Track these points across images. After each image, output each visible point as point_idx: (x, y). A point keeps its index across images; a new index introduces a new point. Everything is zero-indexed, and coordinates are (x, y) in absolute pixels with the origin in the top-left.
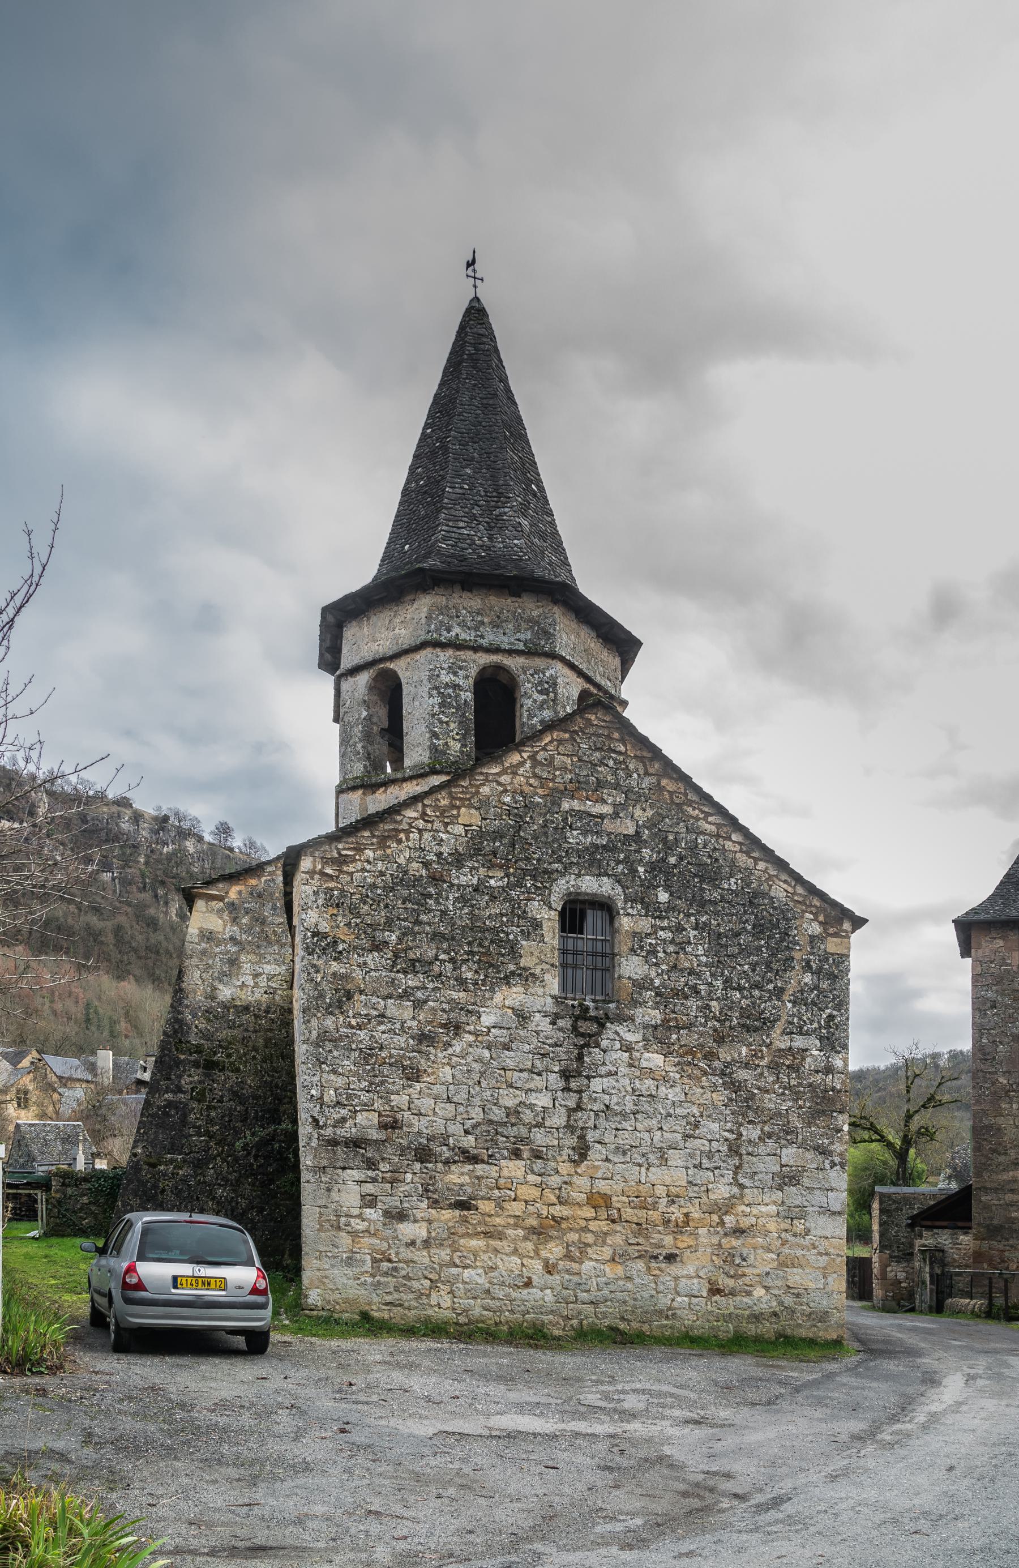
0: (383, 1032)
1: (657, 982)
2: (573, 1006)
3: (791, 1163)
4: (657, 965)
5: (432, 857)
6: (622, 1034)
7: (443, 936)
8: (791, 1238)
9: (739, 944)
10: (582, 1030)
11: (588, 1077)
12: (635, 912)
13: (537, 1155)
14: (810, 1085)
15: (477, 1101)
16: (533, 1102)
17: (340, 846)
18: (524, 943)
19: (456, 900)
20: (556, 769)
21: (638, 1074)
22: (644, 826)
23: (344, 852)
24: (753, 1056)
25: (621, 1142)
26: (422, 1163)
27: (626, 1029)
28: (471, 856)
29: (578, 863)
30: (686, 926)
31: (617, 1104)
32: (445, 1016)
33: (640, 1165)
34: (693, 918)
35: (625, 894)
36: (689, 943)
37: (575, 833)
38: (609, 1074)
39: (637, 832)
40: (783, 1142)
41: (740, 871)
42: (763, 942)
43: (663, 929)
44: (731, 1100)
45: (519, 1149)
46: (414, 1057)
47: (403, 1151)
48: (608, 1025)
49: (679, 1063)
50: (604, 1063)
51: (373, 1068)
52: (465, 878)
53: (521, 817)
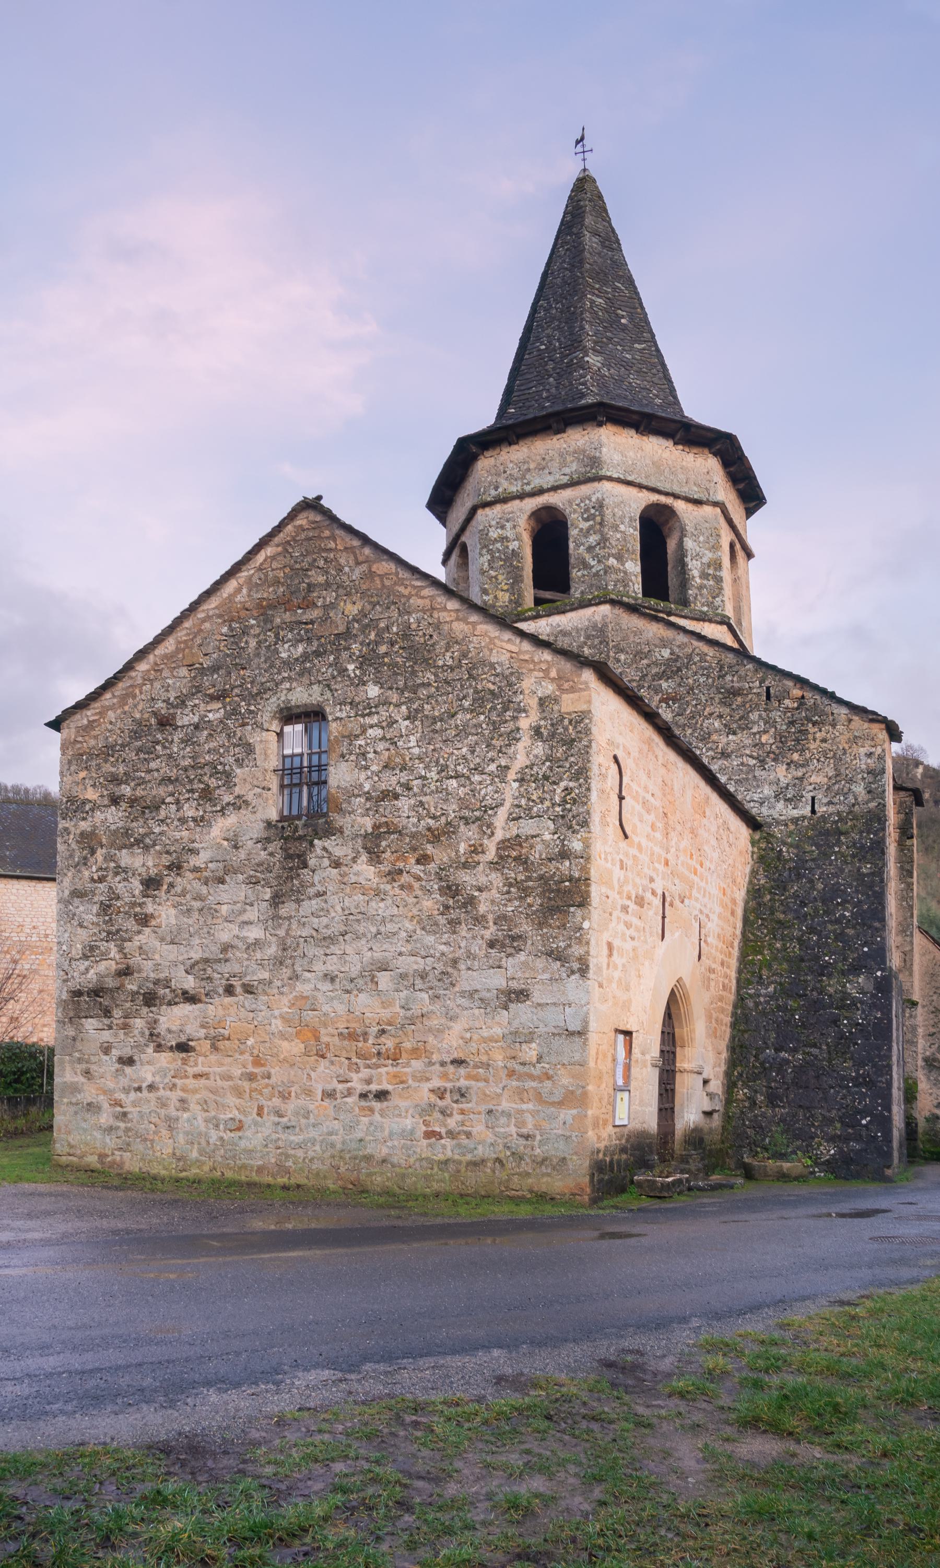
0: (119, 882)
1: (367, 787)
2: (283, 827)
3: (519, 974)
4: (366, 768)
5: (160, 704)
6: (330, 849)
7: (169, 779)
8: (518, 1068)
9: (457, 726)
10: (291, 852)
11: (298, 901)
12: (344, 715)
13: (249, 990)
14: (541, 877)
15: (196, 941)
16: (246, 934)
17: (89, 713)
18: (238, 771)
19: (182, 741)
20: (269, 587)
21: (348, 891)
22: (354, 620)
23: (91, 719)
24: (473, 852)
25: (330, 968)
26: (149, 1007)
27: (334, 843)
28: (193, 695)
29: (289, 679)
30: (397, 718)
31: (327, 927)
32: (169, 858)
33: (348, 992)
34: (404, 708)
35: (334, 698)
36: (402, 736)
37: (286, 646)
38: (319, 895)
39: (348, 628)
40: (509, 950)
41: (457, 642)
42: (482, 717)
43: (372, 727)
44: (447, 907)
45: (231, 986)
46: (144, 903)
47: (134, 994)
48: (316, 841)
49: (390, 873)
50: (313, 885)
51: (110, 919)
52: (186, 719)
53: (236, 644)
